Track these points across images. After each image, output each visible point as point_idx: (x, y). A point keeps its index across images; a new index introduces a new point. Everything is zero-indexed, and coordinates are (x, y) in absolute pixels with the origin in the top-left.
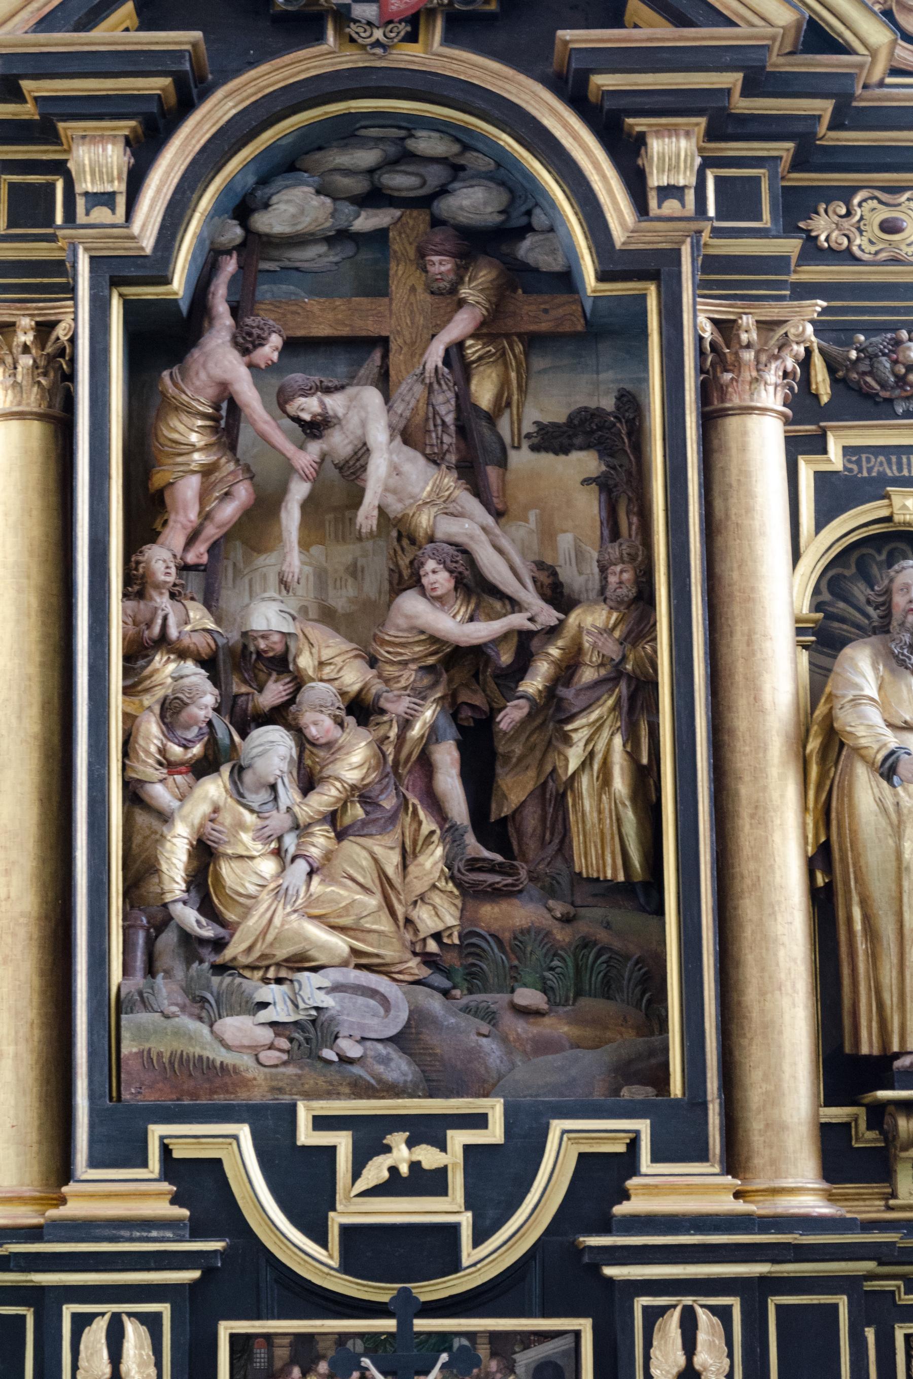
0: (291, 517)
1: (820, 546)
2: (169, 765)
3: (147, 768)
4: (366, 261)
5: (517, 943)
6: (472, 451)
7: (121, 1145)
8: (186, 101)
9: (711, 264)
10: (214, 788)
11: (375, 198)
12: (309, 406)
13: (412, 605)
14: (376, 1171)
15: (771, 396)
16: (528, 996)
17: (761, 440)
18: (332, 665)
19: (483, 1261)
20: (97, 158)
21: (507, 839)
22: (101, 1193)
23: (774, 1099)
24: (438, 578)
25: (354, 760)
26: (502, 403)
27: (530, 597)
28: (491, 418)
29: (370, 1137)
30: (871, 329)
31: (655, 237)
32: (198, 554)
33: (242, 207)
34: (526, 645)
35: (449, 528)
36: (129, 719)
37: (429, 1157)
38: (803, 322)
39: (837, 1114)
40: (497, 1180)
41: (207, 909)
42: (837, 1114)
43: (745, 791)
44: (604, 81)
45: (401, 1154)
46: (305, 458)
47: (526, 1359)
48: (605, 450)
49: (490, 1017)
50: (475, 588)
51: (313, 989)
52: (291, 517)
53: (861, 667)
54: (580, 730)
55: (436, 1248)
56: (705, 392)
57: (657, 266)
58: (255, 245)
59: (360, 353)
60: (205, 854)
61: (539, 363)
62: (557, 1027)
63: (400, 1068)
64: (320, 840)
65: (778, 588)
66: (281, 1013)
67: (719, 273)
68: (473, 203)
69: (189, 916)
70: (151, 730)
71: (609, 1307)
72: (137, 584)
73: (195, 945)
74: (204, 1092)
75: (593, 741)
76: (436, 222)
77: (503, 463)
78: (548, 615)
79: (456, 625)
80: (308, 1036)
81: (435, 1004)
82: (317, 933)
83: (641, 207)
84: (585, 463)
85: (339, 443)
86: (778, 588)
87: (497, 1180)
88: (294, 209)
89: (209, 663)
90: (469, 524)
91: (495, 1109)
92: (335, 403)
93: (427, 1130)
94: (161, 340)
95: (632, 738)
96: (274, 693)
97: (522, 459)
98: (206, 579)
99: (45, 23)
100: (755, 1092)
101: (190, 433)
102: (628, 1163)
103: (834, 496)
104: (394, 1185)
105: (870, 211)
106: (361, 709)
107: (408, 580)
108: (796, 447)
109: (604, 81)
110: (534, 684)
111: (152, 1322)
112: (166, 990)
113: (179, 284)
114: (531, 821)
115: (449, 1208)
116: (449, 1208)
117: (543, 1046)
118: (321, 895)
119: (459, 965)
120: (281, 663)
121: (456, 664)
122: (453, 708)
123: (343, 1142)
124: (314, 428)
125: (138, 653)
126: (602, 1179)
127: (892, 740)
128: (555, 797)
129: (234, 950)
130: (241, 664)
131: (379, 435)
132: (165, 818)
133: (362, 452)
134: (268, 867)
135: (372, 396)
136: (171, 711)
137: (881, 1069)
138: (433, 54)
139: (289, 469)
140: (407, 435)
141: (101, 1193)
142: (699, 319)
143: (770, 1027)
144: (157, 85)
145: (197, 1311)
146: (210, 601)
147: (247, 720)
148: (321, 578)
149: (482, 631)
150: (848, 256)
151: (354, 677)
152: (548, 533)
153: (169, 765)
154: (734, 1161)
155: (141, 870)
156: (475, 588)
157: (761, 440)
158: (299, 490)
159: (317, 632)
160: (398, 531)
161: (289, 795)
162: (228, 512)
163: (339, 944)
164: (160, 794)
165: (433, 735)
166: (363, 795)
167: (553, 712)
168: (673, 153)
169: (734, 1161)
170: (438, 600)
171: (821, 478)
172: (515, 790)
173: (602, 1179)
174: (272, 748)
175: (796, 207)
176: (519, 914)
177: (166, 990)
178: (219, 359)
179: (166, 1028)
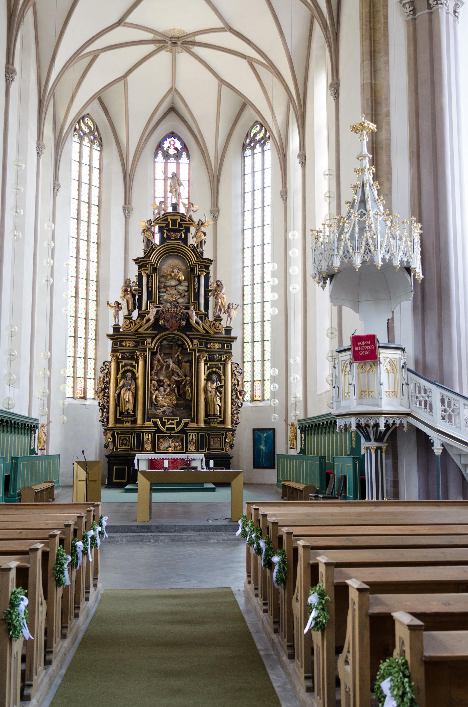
0: (164, 369)
1: (207, 373)
2: (153, 390)
3: (152, 390)
4: (171, 347)
5: (181, 404)
6: (179, 363)
7: (149, 420)
8: (156, 336)
9: (198, 350)
10: (157, 392)
11: (171, 342)
12: (165, 360)
13: (173, 377)
14: (169, 423)
15: (203, 361)
16: (182, 409)
17: (202, 364)
18: (167, 381)
19: (177, 430)
20: (149, 340)
21: (181, 395)
22: (147, 424)
23: (201, 418)
24: (175, 375)
25: (168, 390)
26: (182, 359)
27: (183, 376)
28: (181, 360)
29: (168, 420)
30: (212, 355)
31: (194, 348)
32: (156, 372)
33: (160, 342)
34: (183, 380)
35: (177, 371)
36: (150, 386)
37: (173, 422)
38: (206, 355)
39: (206, 419)
40: (178, 424)
41: (156, 402)
42: (206, 419)
43: (199, 393)
44: (190, 336)
45: (171, 421)
46: (165, 364)
47: (180, 438)
48: (190, 363)
49: (178, 410)
50: (178, 375)
51: (165, 408)
52: (164, 369)
53: (209, 384)
54: (187, 387)
55: (173, 429)
56: (198, 360)
58: (161, 345)
59: (170, 355)
60: (156, 397)
61: (185, 355)
62: (184, 411)
63: (171, 414)
64: (165, 396)
65: (203, 376)
66: (162, 410)
67: (199, 351)
68: (180, 342)
69: (155, 402)
70: (152, 387)
71: (187, 434)
72: (151, 375)
73: (156, 405)
74: (156, 416)
75: (188, 388)
76: (177, 344)
77: (181, 364)
78: (184, 378)
79: (176, 379)
80: (164, 412)
81: (174, 409)
82: (165, 404)
83: (193, 346)
84: (188, 364)
85: (168, 363)
86: (203, 376)
87: (178, 424)
88: (165, 343)
89: (157, 381)
90: (178, 370)
91: (178, 418)
92: (168, 360)
93: (173, 420)
94: (154, 354)
95: (191, 388)
96: (162, 384)
97: (183, 364)
98: (157, 374)
99: (145, 330)
100: (199, 417)
101: (156, 362)
102: (189, 423)
103: (208, 368)
104: (170, 424)
105: (212, 344)
106: (169, 385)
107: (173, 375)
108: (205, 364)
109: (190, 336)
110: (183, 384)
111: (151, 434)
112: (153, 408)
113: (155, 350)
114: (183, 394)
115: (174, 426)
116: (174, 426)
117: (183, 413)
118: (164, 400)
119: (176, 406)
120: (163, 381)
121: (176, 382)
122: (176, 385)
123: (166, 420)
124: (166, 362)
125: (151, 380)
126: (186, 424)
127: (211, 390)
128: (185, 392)
129: (158, 405)
130: (159, 381)
131: (171, 363)
132: (153, 394)
133: (170, 364)
134: (161, 398)
135: (171, 360)
136: (154, 386)
138: (176, 332)
139: (163, 365)
140: (174, 362)
141: (147, 424)
142: (197, 355)
143: (201, 412)
144: (154, 335)
145: (154, 434)
146: (157, 376)
147: (160, 386)
148: (166, 373)
149: (179, 379)
150: (210, 348)
151: (168, 383)
152: (185, 370)
153: (153, 390)
154: (197, 423)
155: (151, 398)
156: (178, 375)
157: (202, 364)
158: (164, 367)
159: (166, 379)
160: (172, 370)
161: (163, 392)
162: (159, 368)
163: (166, 404)
164: (153, 392)
165: (175, 387)
166: (169, 392)
167: (185, 386)
168: (195, 341)
169: (197, 422)
170: (176, 377)
171: (207, 367)
172: (181, 392)
173: (186, 424)
174: (162, 389)
175: (206, 344)
176: (181, 402)
177: (153, 408)
178: (158, 356)
179: (153, 411)
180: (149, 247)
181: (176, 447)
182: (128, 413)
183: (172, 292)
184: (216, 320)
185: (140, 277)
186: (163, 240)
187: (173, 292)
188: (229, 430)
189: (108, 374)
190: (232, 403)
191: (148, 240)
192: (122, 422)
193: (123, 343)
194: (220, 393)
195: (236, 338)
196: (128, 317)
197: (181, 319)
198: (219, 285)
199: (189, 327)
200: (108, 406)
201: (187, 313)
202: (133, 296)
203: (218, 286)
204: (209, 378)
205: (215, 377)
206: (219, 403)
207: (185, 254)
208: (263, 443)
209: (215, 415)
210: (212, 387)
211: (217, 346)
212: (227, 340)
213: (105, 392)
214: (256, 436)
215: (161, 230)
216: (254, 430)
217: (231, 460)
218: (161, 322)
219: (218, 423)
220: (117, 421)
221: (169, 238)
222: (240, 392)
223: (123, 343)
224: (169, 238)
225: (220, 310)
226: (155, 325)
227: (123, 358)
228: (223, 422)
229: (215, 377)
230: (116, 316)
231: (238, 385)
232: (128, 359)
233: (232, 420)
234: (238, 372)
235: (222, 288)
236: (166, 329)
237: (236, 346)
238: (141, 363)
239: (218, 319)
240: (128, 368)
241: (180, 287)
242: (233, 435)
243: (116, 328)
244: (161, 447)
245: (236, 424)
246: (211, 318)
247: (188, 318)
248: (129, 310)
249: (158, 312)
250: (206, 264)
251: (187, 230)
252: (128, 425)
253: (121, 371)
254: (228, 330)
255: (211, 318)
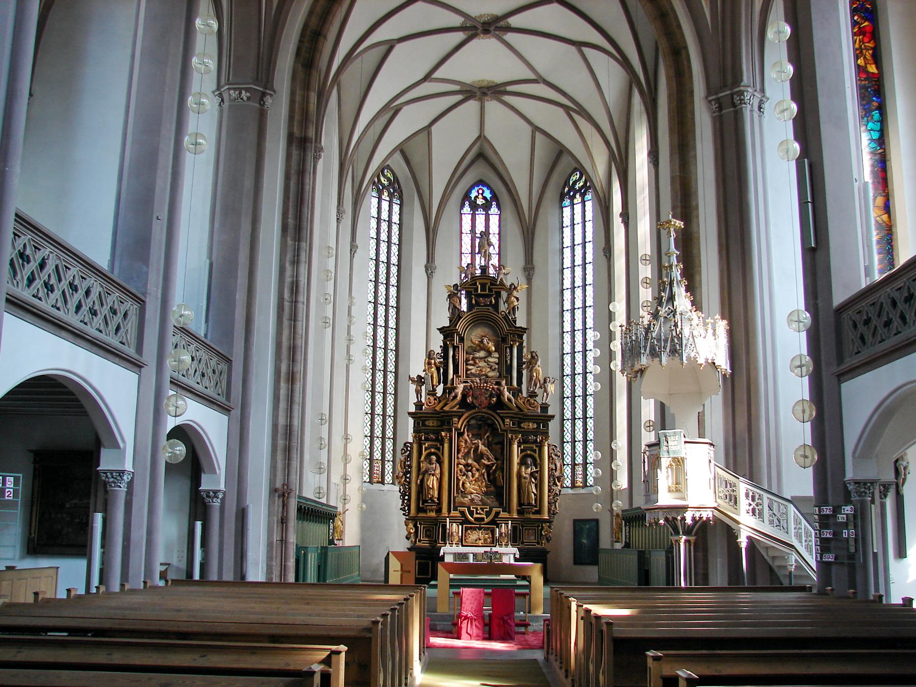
7: (455, 509)
17: (515, 446)
25: (477, 475)
34: (493, 465)
50: (488, 459)
57: (506, 431)
60: (463, 484)
65: (516, 460)
68: (489, 421)
74: (463, 505)
75: (498, 473)
80: (472, 500)
84: (499, 446)
86: (516, 460)
88: (473, 422)
90: (489, 453)
103: (522, 451)
106: (478, 470)
108: (518, 446)
126: (498, 513)
130: (467, 465)
137: (523, 505)
147: (468, 471)
155: (458, 485)
157: (515, 446)
172: (492, 477)
173: (498, 513)
175: (519, 423)
178: (466, 436)
179: (460, 499)
180: (456, 315)
181: (485, 540)
182: (433, 501)
183: (480, 364)
184: (530, 396)
185: (445, 349)
186: (470, 306)
187: (482, 364)
188: (545, 521)
189: (410, 456)
190: (549, 491)
191: (455, 307)
192: (425, 511)
193: (427, 423)
194: (535, 479)
195: (553, 417)
196: (432, 393)
197: (491, 396)
198: (534, 358)
199: (500, 404)
200: (410, 493)
201: (499, 389)
202: (438, 369)
203: (533, 357)
204: (522, 462)
205: (529, 461)
206: (534, 490)
207: (495, 322)
208: (585, 536)
209: (530, 504)
210: (526, 472)
211: (532, 426)
212: (544, 419)
213: (406, 477)
214: (577, 528)
215: (468, 296)
216: (575, 521)
217: (548, 556)
218: (469, 400)
219: (533, 513)
220: (419, 509)
221: (478, 304)
222: (559, 478)
223: (427, 423)
224: (478, 304)
225: (535, 385)
226: (463, 403)
227: (427, 439)
228: (539, 512)
229: (529, 461)
230: (418, 392)
231: (556, 470)
232: (432, 440)
233: (549, 510)
234: (556, 455)
235: (537, 360)
236: (474, 407)
237: (553, 426)
238: (446, 445)
239: (533, 395)
240: (433, 450)
241: (490, 359)
242: (549, 527)
243: (419, 405)
244: (469, 540)
245: (554, 514)
246: (525, 394)
247: (500, 395)
248: (433, 386)
249: (465, 387)
250: (520, 333)
251: (498, 295)
252: (433, 514)
253: (424, 453)
254: (545, 408)
255: (525, 394)
